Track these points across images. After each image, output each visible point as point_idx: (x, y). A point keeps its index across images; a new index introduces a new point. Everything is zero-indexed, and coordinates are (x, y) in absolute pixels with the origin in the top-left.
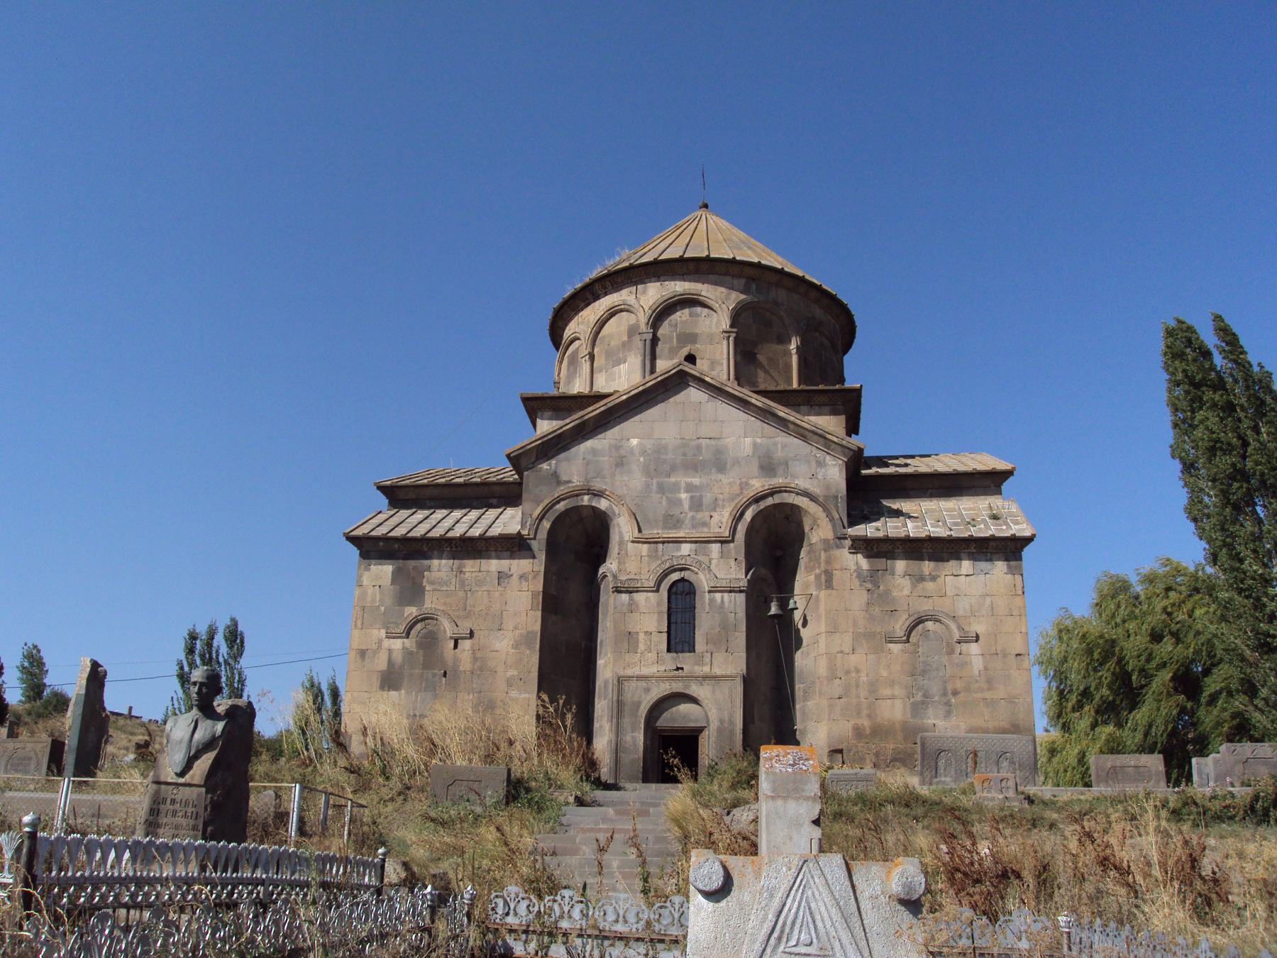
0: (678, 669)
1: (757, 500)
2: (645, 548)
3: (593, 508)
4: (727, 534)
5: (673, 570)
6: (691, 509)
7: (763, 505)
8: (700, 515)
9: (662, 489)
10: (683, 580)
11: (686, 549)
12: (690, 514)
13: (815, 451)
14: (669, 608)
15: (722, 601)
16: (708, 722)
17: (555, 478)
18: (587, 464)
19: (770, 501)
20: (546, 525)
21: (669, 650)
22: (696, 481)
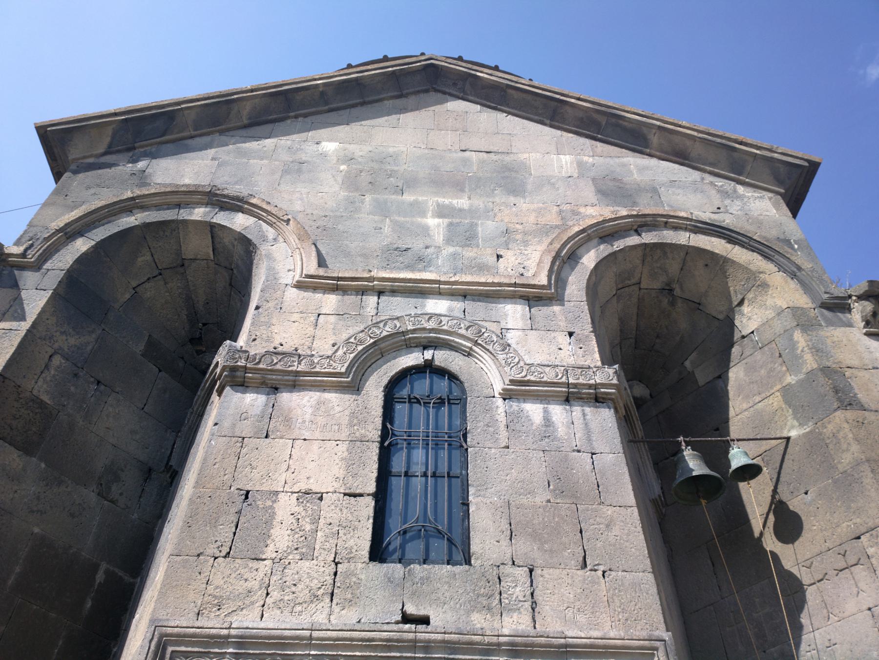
0: (407, 619)
1: (604, 233)
2: (330, 301)
3: (213, 229)
4: (543, 280)
5: (404, 342)
6: (449, 241)
7: (619, 245)
8: (469, 253)
9: (382, 210)
10: (428, 368)
11: (437, 306)
12: (451, 249)
13: (709, 178)
14: (385, 433)
15: (548, 421)
17: (142, 178)
18: (219, 165)
19: (633, 240)
20: (82, 245)
21: (378, 552)
22: (462, 202)
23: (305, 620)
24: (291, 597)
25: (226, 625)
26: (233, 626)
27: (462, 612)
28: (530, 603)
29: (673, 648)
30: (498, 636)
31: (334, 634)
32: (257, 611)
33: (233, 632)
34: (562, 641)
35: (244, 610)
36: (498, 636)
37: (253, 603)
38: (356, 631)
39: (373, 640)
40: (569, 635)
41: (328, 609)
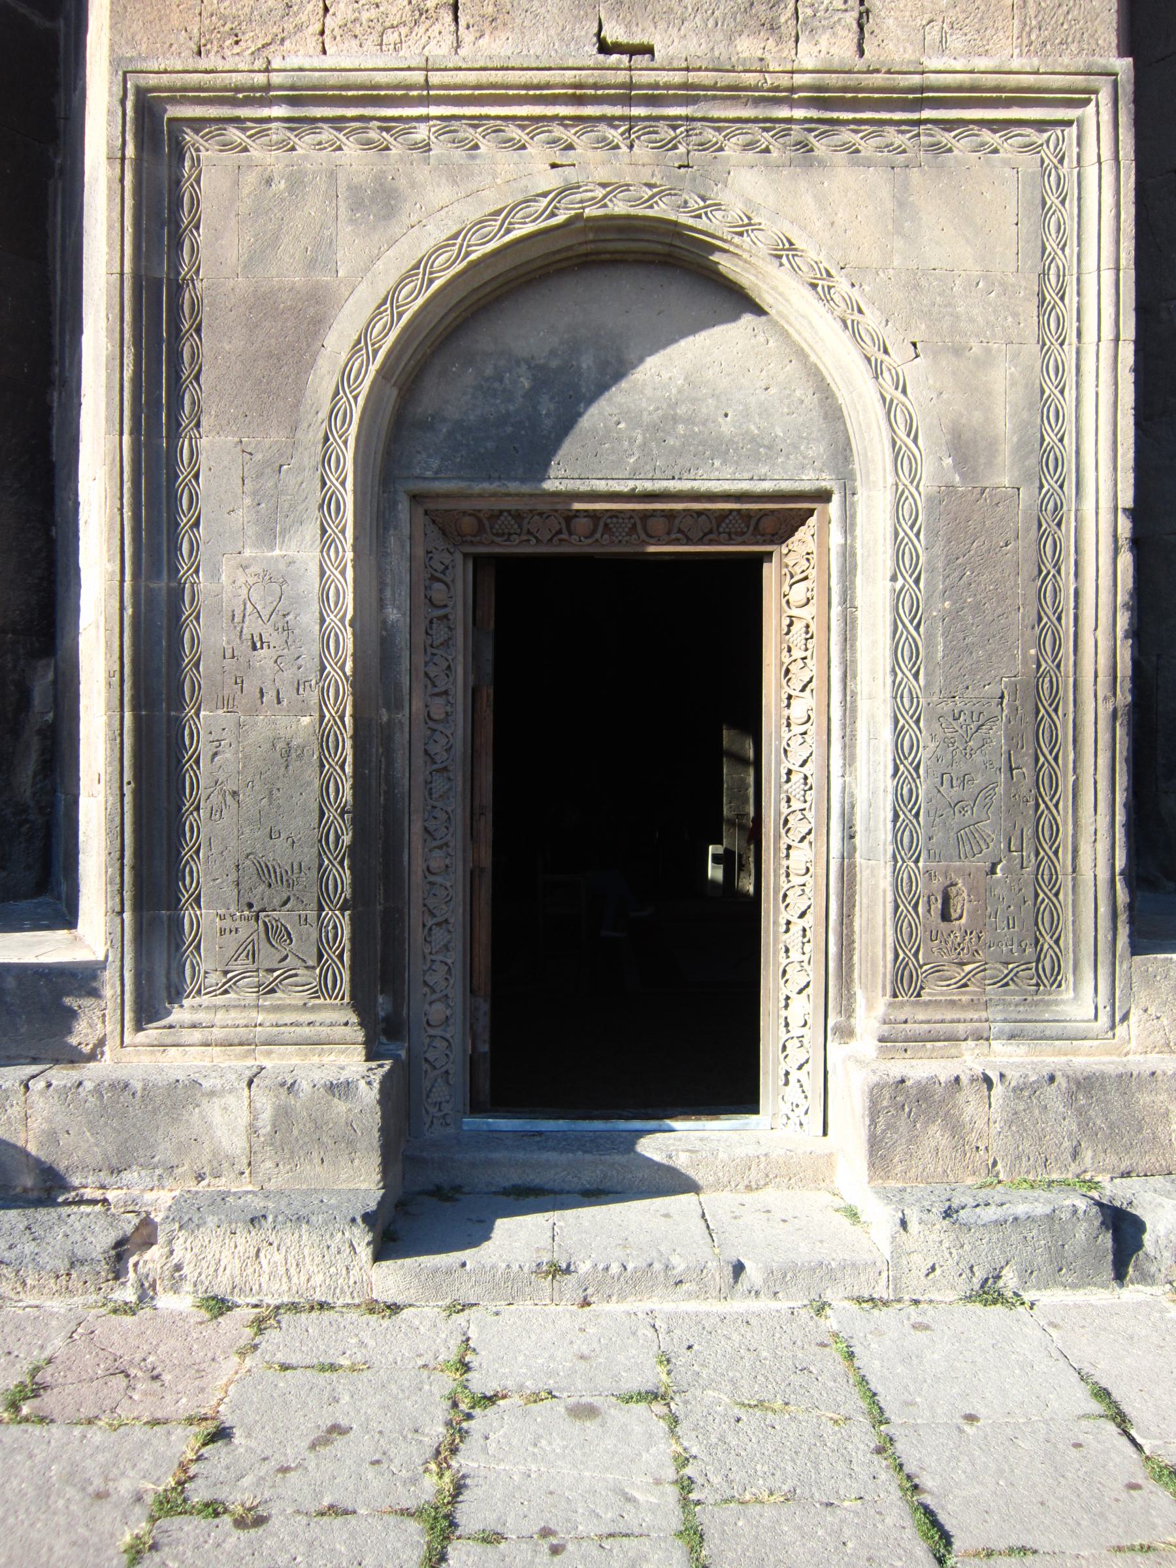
16: (842, 454)
23: (410, 54)
24: (374, 13)
25: (259, 64)
26: (274, 65)
27: (719, 36)
28: (856, 14)
29: (1130, 88)
30: (792, 72)
31: (472, 77)
32: (313, 43)
33: (276, 78)
34: (916, 79)
35: (287, 43)
36: (792, 72)
37: (299, 28)
38: (513, 69)
39: (548, 86)
40: (932, 68)
41: (452, 38)
